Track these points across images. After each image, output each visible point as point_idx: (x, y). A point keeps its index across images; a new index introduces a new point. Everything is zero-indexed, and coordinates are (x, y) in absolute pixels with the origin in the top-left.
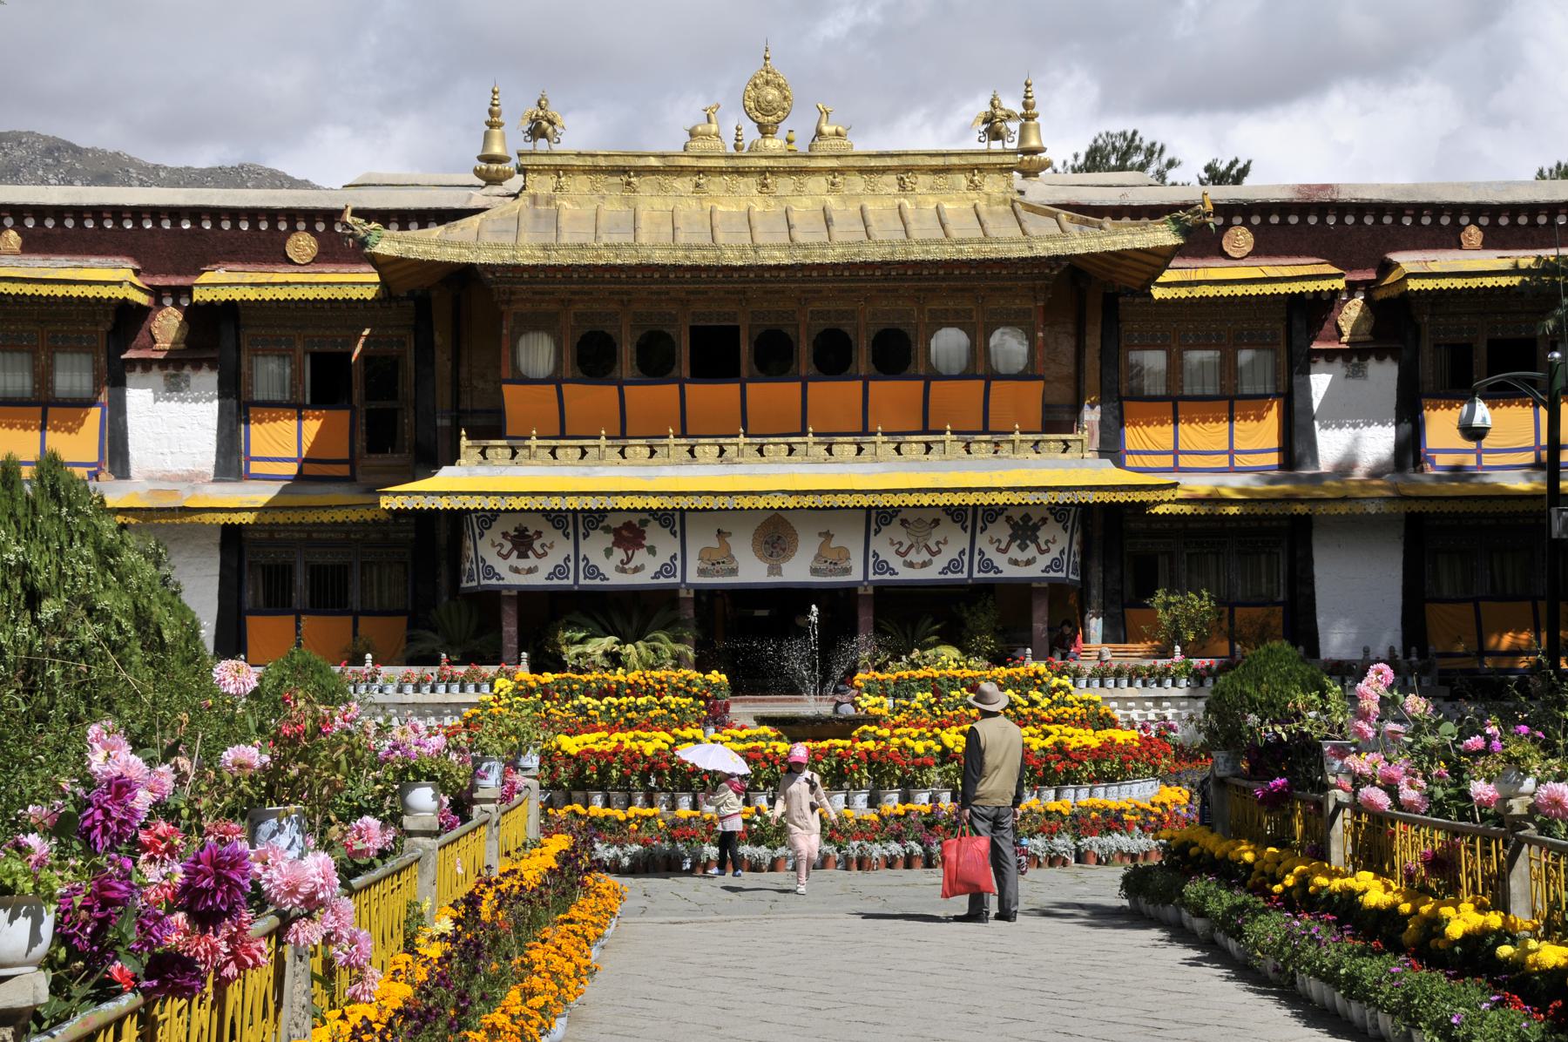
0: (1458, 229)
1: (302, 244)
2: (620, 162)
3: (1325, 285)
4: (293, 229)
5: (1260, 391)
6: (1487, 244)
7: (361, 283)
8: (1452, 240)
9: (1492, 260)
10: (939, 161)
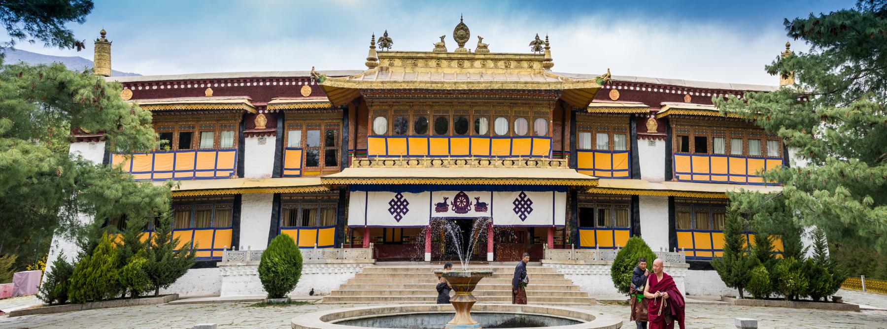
0: (683, 96)
1: (306, 90)
2: (411, 55)
3: (643, 111)
4: (303, 85)
5: (621, 149)
6: (692, 102)
7: (323, 101)
8: (681, 98)
9: (694, 106)
10: (518, 57)
